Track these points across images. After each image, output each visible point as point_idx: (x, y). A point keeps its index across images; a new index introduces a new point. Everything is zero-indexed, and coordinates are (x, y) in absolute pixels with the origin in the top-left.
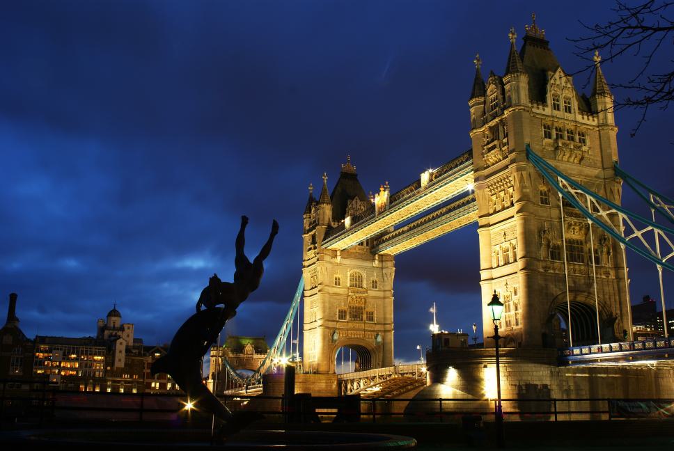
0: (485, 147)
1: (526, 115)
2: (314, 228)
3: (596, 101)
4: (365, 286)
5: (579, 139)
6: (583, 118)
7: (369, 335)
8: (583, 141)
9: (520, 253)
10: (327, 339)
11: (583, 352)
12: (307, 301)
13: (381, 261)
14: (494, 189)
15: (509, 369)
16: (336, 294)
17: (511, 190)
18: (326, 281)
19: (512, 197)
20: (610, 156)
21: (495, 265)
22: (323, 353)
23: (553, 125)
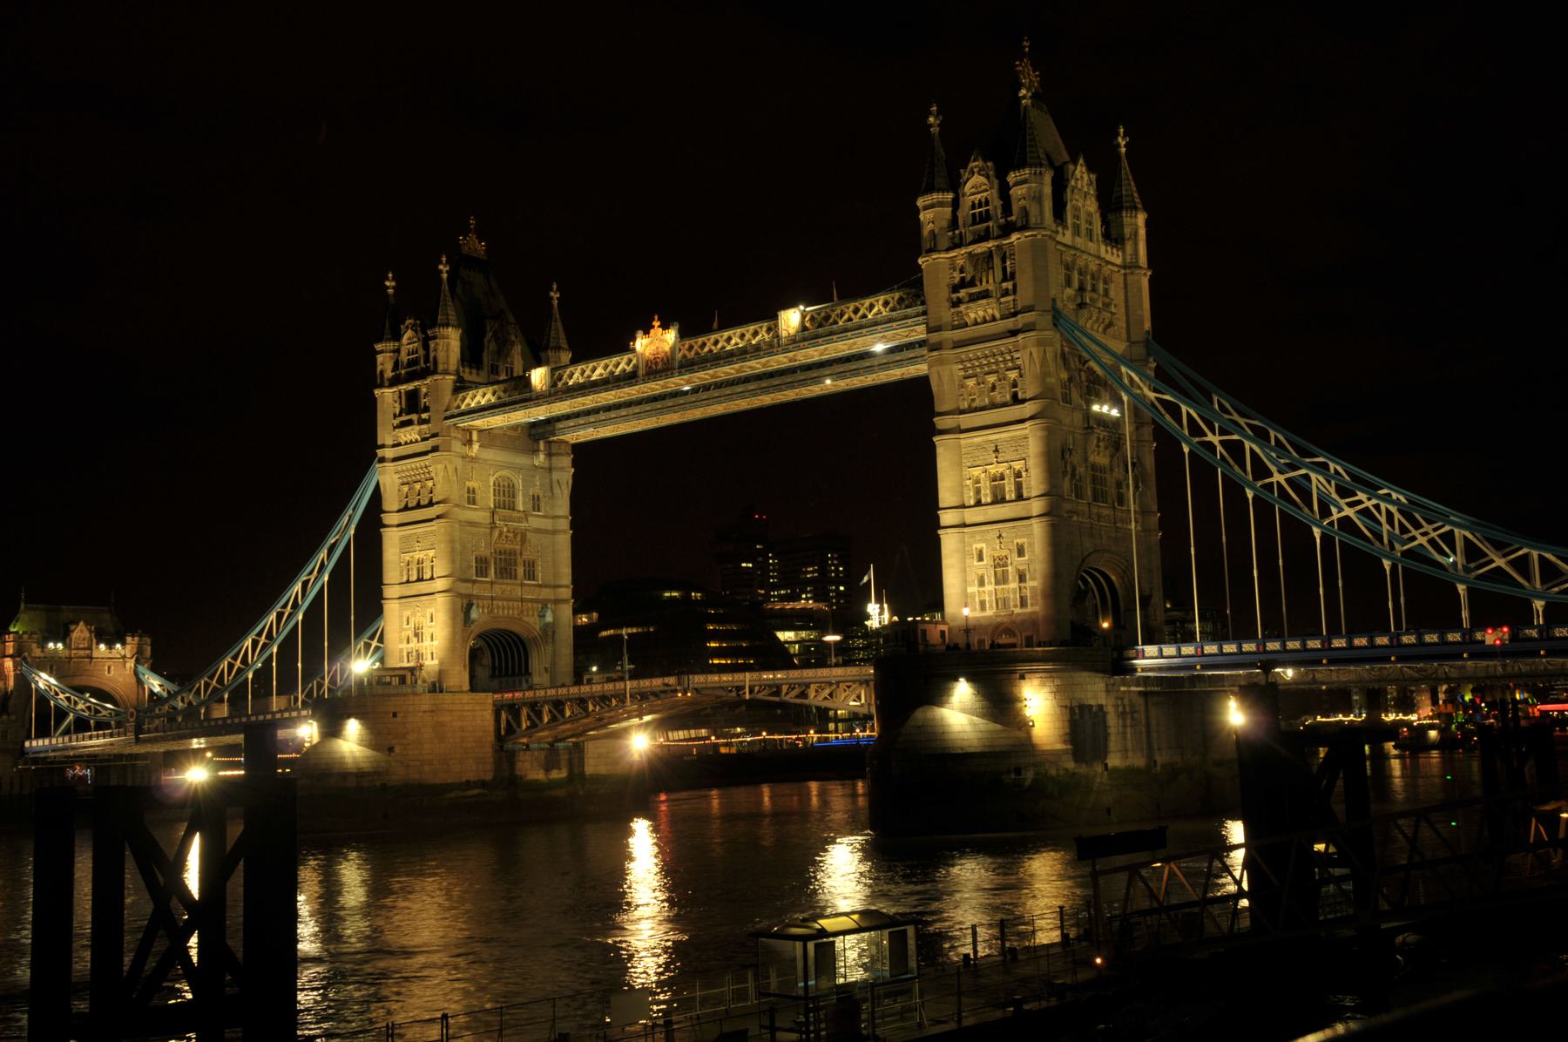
3: (1122, 222)
6: (1107, 251)
12: (392, 540)
13: (549, 455)
14: (973, 367)
15: (1058, 682)
16: (471, 524)
17: (1013, 375)
18: (456, 494)
21: (972, 502)
22: (452, 648)
23: (1074, 262)
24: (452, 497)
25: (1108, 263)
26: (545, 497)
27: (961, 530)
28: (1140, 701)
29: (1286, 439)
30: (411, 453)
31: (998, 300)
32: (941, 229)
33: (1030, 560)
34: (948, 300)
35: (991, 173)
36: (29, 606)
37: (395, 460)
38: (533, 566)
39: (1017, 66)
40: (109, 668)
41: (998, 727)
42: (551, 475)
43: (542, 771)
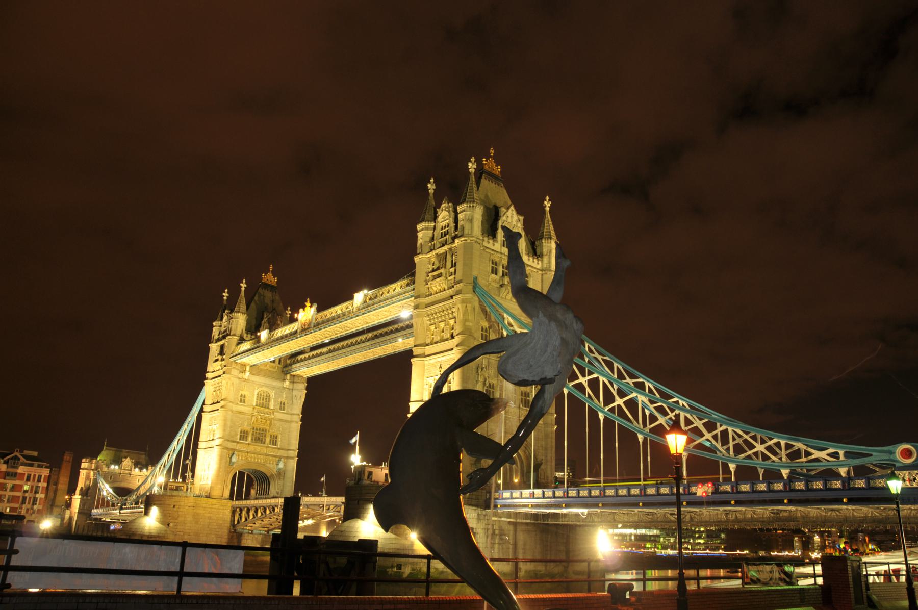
0: (430, 274)
1: (477, 246)
2: (224, 337)
3: (542, 246)
6: (529, 260)
7: (270, 461)
10: (224, 461)
11: (514, 496)
13: (293, 382)
14: (434, 319)
16: (240, 413)
17: (452, 322)
18: (231, 398)
19: (453, 329)
22: (218, 475)
23: (500, 261)
26: (288, 403)
28: (511, 528)
31: (447, 278)
32: (426, 242)
35: (451, 209)
36: (107, 448)
38: (276, 438)
40: (139, 480)
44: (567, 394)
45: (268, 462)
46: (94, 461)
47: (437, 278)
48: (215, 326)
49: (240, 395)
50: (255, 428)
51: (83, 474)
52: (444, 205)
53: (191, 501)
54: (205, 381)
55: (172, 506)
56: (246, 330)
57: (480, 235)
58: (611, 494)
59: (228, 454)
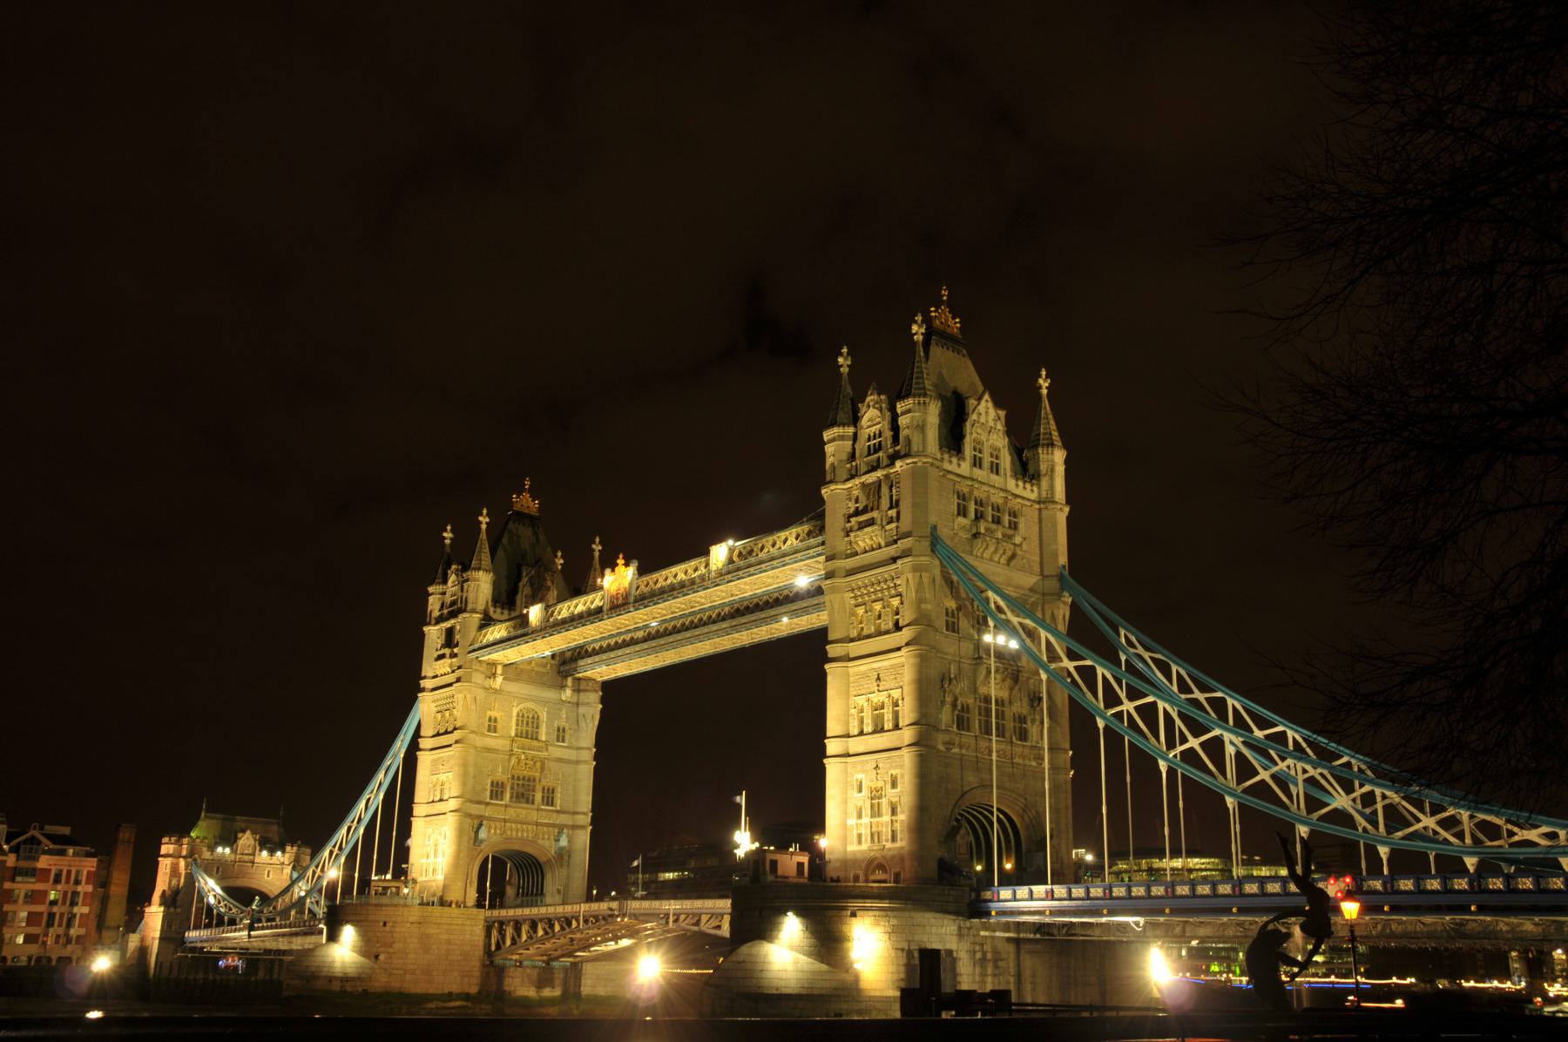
0: (853, 520)
1: (934, 473)
2: (453, 615)
3: (1038, 458)
4: (543, 737)
5: (993, 516)
6: (1017, 485)
8: (1014, 526)
9: (908, 713)
10: (466, 838)
12: (424, 760)
13: (577, 690)
14: (862, 596)
15: (894, 922)
16: (489, 750)
17: (895, 602)
18: (473, 724)
19: (897, 614)
20: (1055, 555)
21: (856, 732)
22: (456, 864)
23: (971, 492)
24: (468, 724)
25: (1016, 496)
26: (570, 729)
27: (843, 760)
28: (1011, 948)
29: (1188, 674)
30: (443, 683)
31: (883, 527)
32: (841, 461)
33: (902, 792)
34: (843, 530)
35: (884, 405)
36: (209, 814)
37: (434, 689)
38: (553, 792)
39: (932, 312)
40: (269, 873)
41: (824, 967)
42: (578, 709)
43: (533, 988)
44: (1104, 729)
45: (541, 836)
46: (185, 840)
47: (866, 526)
48: (432, 594)
49: (487, 719)
50: (516, 776)
51: (165, 865)
52: (872, 397)
53: (415, 914)
54: (419, 695)
55: (382, 924)
56: (492, 601)
57: (937, 450)
58: (1184, 893)
59: (472, 826)
